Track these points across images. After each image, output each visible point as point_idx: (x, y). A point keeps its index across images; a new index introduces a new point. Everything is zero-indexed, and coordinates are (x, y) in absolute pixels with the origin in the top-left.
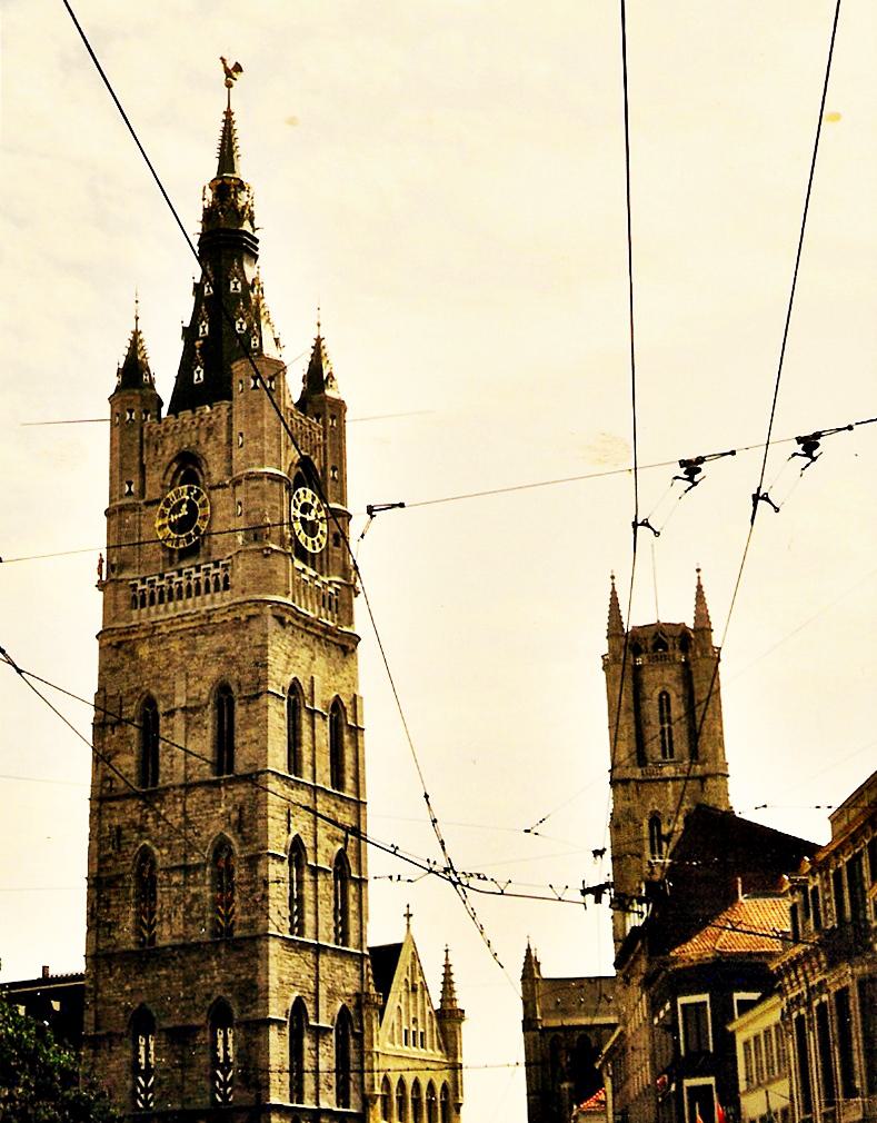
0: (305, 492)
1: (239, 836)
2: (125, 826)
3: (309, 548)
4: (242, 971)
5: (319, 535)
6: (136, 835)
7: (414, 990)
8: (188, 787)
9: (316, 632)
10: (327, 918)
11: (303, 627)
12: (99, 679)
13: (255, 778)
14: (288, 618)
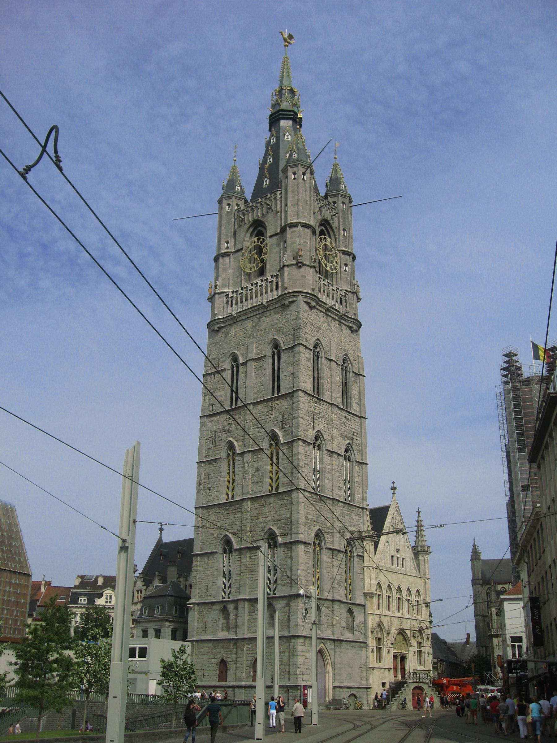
0: (325, 238)
2: (218, 430)
4: (282, 512)
5: (334, 263)
6: (226, 435)
8: (255, 404)
9: (332, 315)
11: (324, 311)
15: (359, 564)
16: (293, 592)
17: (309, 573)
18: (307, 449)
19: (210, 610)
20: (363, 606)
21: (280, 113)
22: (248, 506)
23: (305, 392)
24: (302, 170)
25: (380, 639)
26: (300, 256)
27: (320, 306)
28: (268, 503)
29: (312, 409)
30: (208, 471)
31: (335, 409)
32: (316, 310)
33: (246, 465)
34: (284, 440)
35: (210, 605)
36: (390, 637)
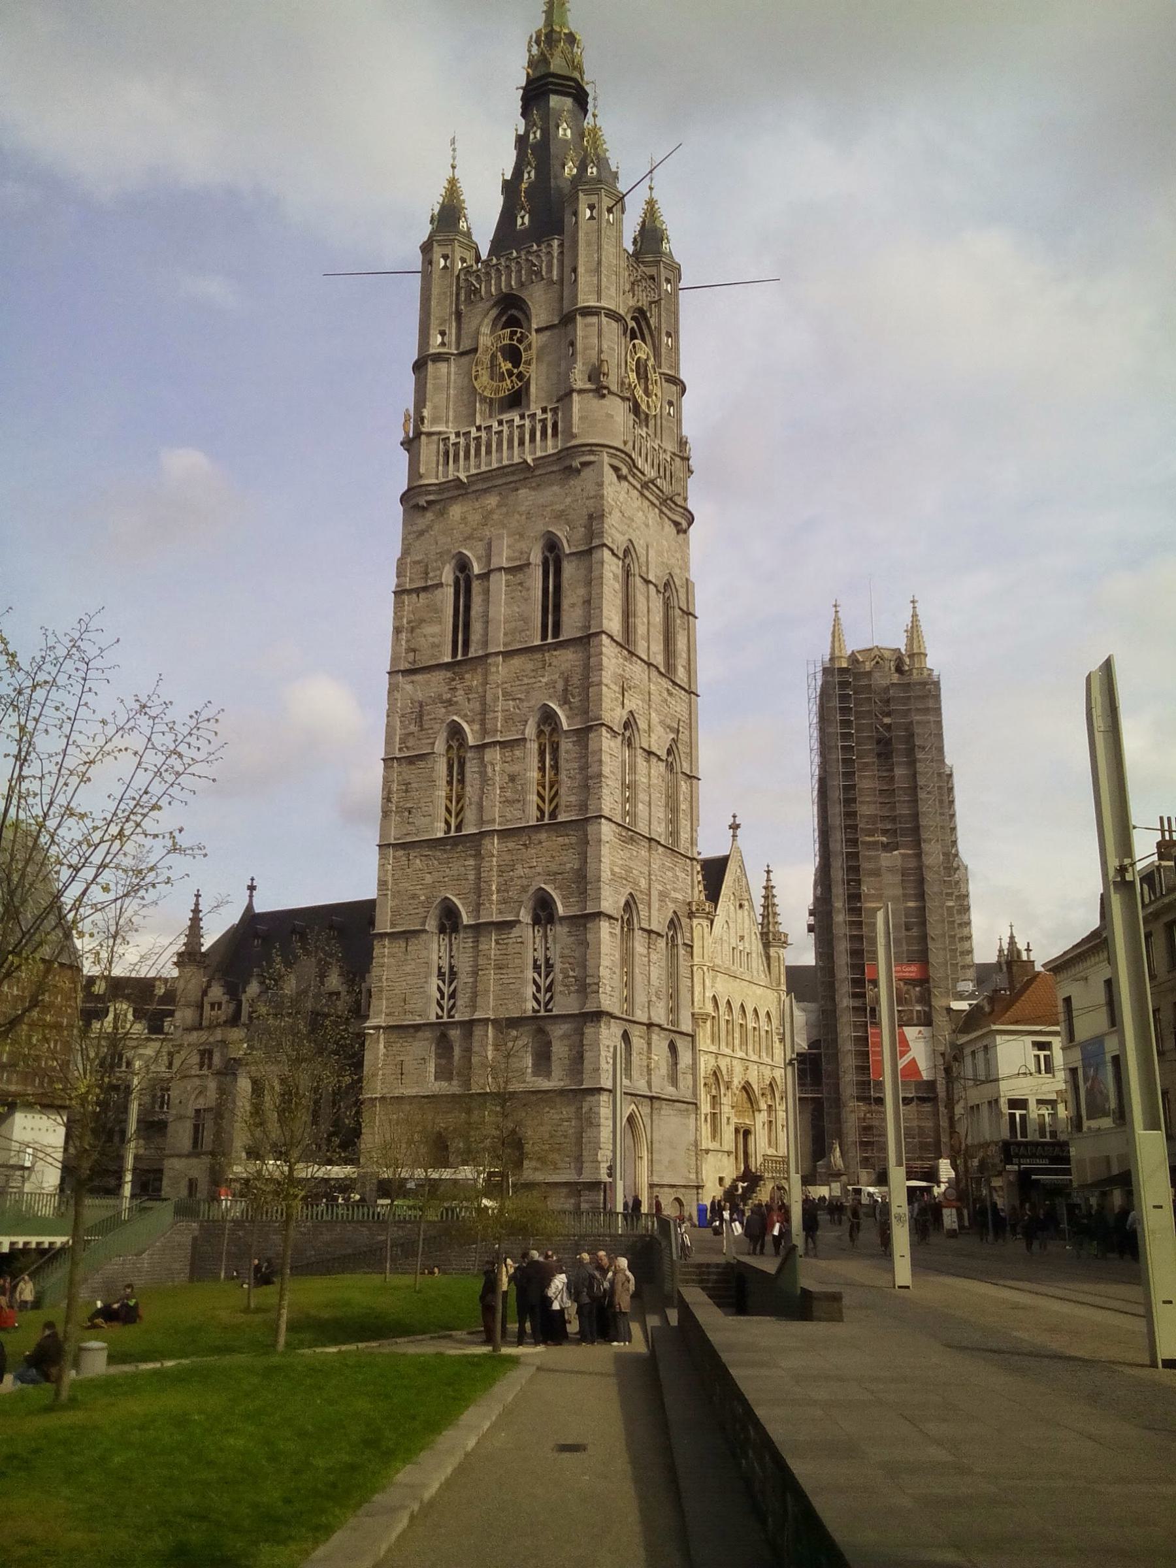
1: (567, 707)
2: (429, 701)
3: (644, 407)
4: (565, 859)
6: (444, 710)
7: (741, 906)
8: (508, 654)
9: (651, 497)
10: (659, 813)
11: (639, 486)
12: (403, 544)
13: (587, 640)
14: (625, 471)
15: (685, 960)
16: (590, 1007)
17: (614, 973)
18: (612, 744)
19: (410, 1040)
20: (692, 1036)
21: (551, 79)
22: (494, 845)
23: (611, 637)
24: (607, 202)
25: (714, 1097)
26: (604, 374)
27: (634, 476)
28: (536, 842)
29: (620, 671)
30: (407, 777)
31: (654, 673)
32: (627, 483)
33: (489, 769)
34: (569, 725)
35: (412, 1030)
36: (729, 1094)
